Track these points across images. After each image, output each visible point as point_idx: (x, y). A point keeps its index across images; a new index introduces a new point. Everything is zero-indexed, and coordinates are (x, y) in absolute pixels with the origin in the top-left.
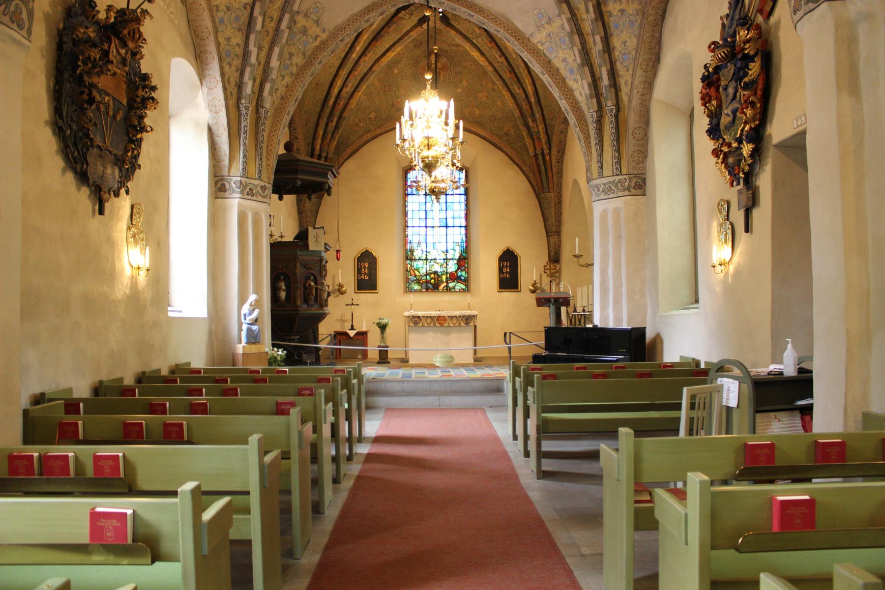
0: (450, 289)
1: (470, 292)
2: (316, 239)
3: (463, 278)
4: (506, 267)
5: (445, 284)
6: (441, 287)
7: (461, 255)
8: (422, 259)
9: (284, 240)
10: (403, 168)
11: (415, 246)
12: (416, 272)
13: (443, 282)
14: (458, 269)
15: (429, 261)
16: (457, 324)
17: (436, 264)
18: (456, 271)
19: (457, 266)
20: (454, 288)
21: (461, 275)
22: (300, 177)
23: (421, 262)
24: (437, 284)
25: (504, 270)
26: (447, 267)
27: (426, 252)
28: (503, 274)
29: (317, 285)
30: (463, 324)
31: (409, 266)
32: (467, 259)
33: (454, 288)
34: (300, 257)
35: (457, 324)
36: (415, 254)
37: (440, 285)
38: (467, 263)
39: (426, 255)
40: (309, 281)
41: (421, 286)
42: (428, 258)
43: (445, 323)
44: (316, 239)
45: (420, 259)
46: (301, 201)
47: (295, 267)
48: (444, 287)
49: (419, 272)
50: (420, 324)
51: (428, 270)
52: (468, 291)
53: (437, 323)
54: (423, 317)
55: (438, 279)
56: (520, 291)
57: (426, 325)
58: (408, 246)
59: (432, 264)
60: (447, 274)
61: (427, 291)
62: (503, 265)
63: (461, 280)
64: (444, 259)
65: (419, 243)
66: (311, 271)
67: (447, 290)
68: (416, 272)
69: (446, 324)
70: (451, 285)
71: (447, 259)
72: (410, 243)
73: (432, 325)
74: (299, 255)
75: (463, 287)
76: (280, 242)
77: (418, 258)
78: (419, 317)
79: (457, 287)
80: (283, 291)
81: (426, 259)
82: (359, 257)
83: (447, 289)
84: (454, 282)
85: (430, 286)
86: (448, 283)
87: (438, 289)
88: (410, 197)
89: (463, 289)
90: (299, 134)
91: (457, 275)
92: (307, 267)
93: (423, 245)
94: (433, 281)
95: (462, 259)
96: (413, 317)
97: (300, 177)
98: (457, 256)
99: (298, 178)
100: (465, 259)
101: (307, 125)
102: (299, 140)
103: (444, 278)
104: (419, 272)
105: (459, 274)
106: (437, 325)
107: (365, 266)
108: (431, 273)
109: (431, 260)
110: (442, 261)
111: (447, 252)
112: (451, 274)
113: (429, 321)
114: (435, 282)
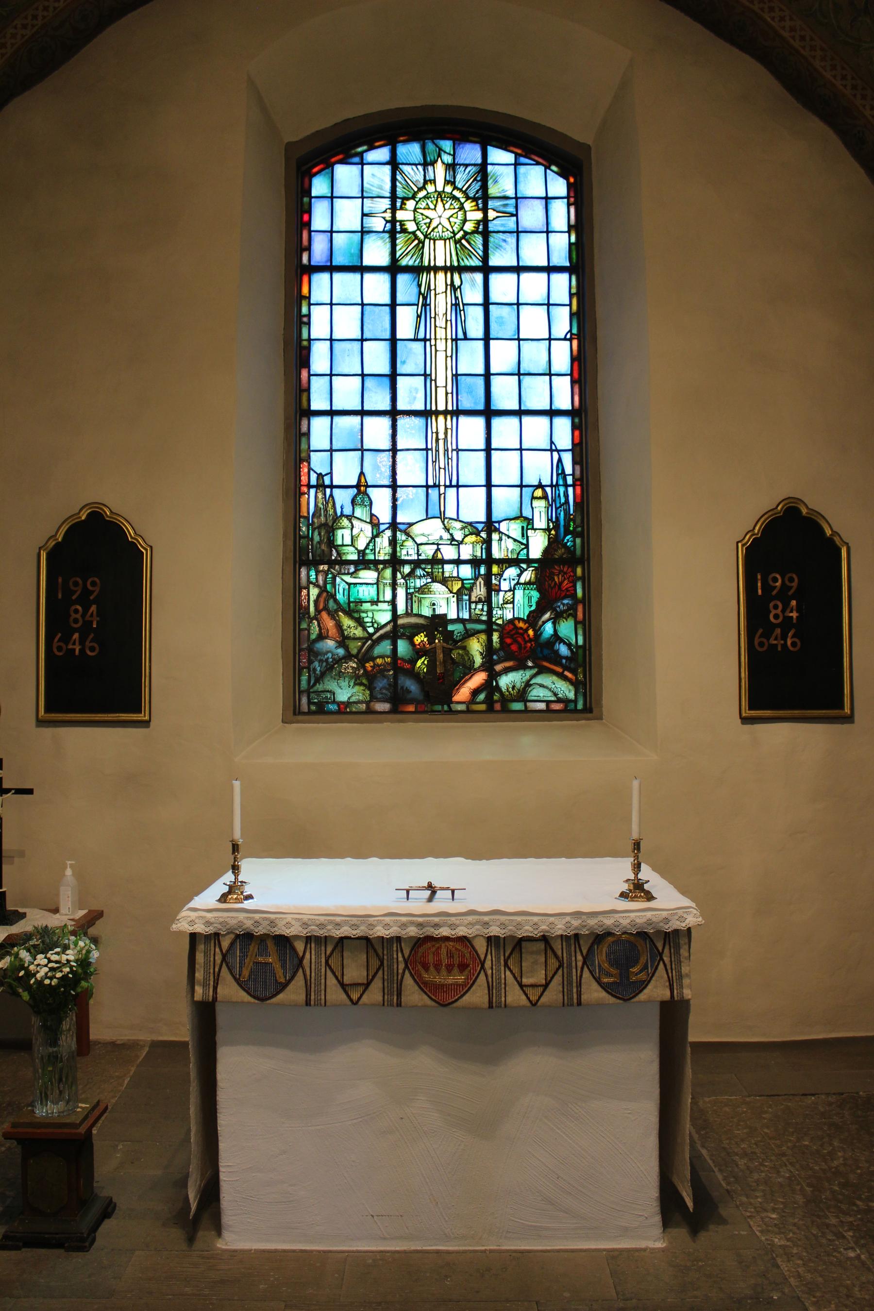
0: (506, 700)
1: (600, 718)
3: (563, 650)
4: (784, 596)
5: (479, 678)
6: (463, 693)
7: (554, 544)
8: (376, 562)
10: (289, 146)
11: (343, 498)
12: (347, 622)
13: (469, 670)
14: (541, 607)
15: (407, 569)
16: (553, 994)
17: (437, 587)
18: (533, 618)
19: (535, 595)
20: (522, 695)
21: (556, 636)
23: (369, 575)
24: (443, 676)
25: (774, 614)
26: (488, 600)
27: (394, 525)
28: (767, 635)
30: (593, 992)
31: (314, 592)
32: (583, 560)
33: (522, 695)
35: (553, 994)
36: (343, 536)
37: (457, 684)
38: (583, 578)
39: (393, 542)
41: (370, 687)
42: (403, 554)
43: (467, 987)
45: (363, 563)
48: (475, 692)
49: (360, 622)
50: (295, 993)
51: (401, 608)
52: (588, 709)
53: (408, 981)
54: (308, 939)
55: (447, 652)
56: (849, 719)
57: (335, 994)
58: (311, 500)
59: (419, 583)
60: (489, 633)
61: (394, 711)
62: (767, 588)
63: (556, 658)
64: (474, 562)
65: (361, 488)
67: (490, 709)
68: (347, 622)
69: (477, 996)
70: (505, 681)
71: (489, 561)
72: (320, 486)
73: (374, 994)
75: (565, 690)
77: (354, 557)
78: (283, 942)
79: (536, 693)
81: (395, 562)
82: (58, 545)
83: (489, 701)
84: (525, 667)
85: (412, 686)
86: (493, 676)
87: (447, 698)
88: (321, 281)
89: (565, 701)
91: (538, 634)
93: (381, 500)
94: (421, 663)
95: (561, 561)
96: (245, 938)
98: (538, 545)
100: (572, 560)
103: (476, 647)
104: (360, 622)
105: (548, 629)
106: (412, 994)
107: (86, 592)
108: (416, 629)
109: (417, 564)
110: (466, 571)
111: (490, 526)
112: (510, 628)
113: (355, 972)
114: (431, 665)
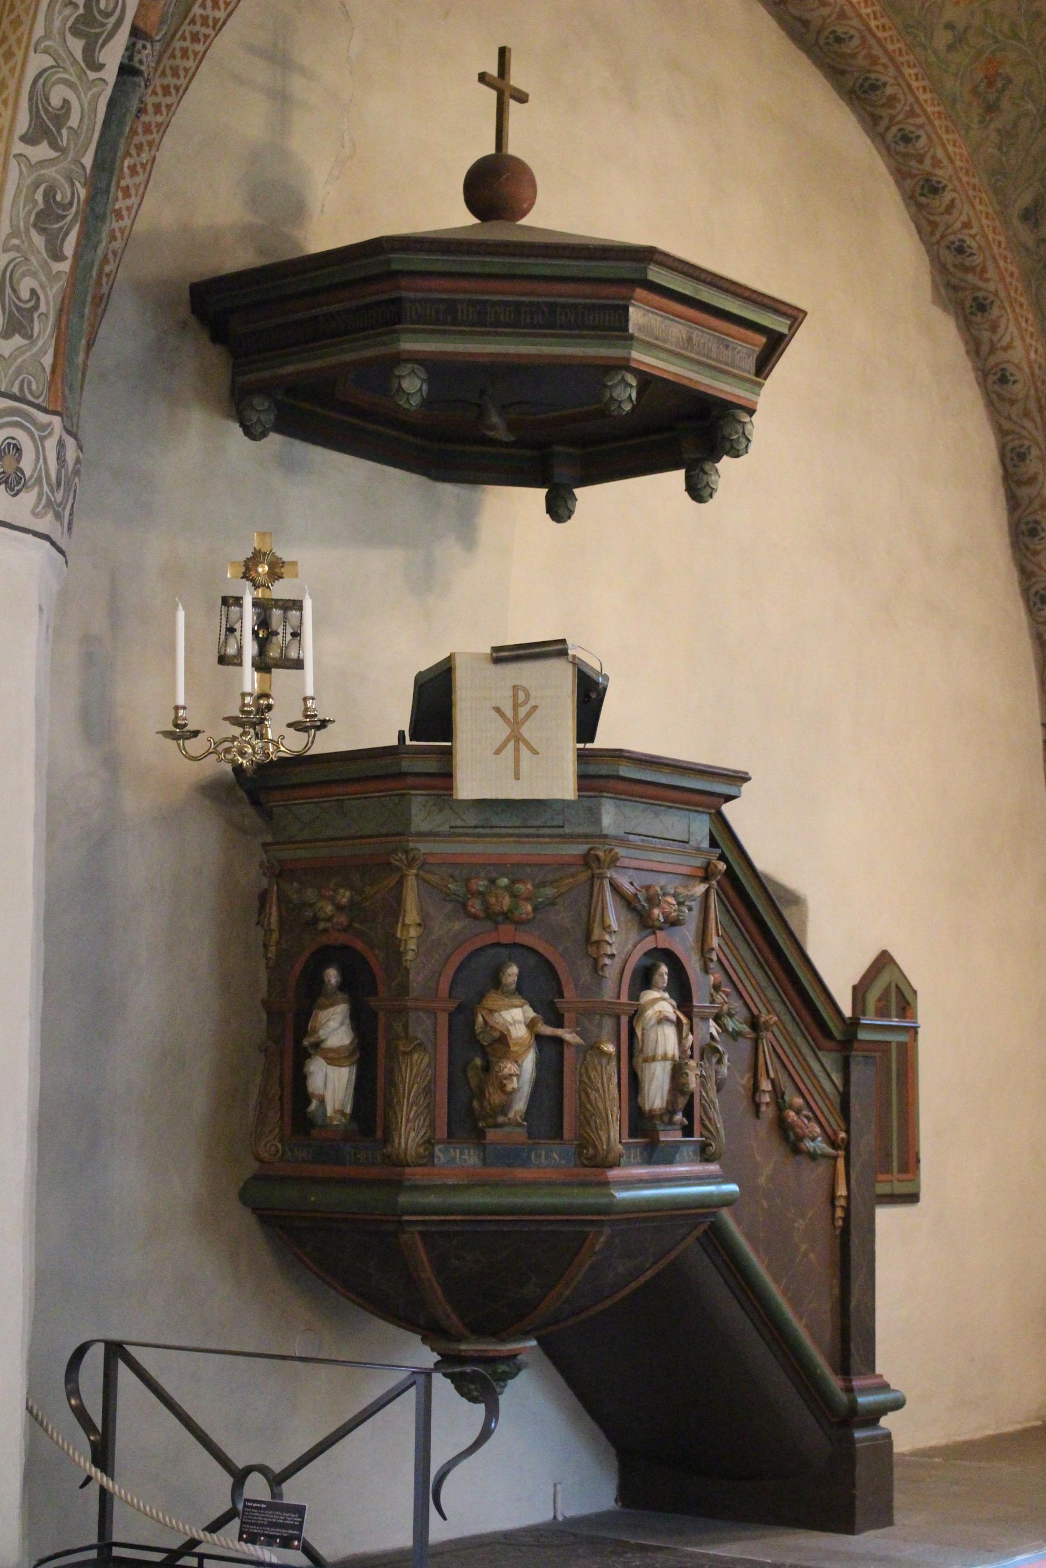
2: (515, 724)
9: (325, 743)
22: (409, 344)
29: (560, 1025)
34: (424, 847)
40: (493, 999)
44: (515, 724)
46: (1033, 532)
47: (395, 907)
66: (507, 933)
74: (423, 835)
76: (300, 760)
80: (334, 1058)
90: (936, 163)
92: (475, 906)
97: (409, 344)
99: (399, 359)
101: (991, 108)
102: (948, 196)
